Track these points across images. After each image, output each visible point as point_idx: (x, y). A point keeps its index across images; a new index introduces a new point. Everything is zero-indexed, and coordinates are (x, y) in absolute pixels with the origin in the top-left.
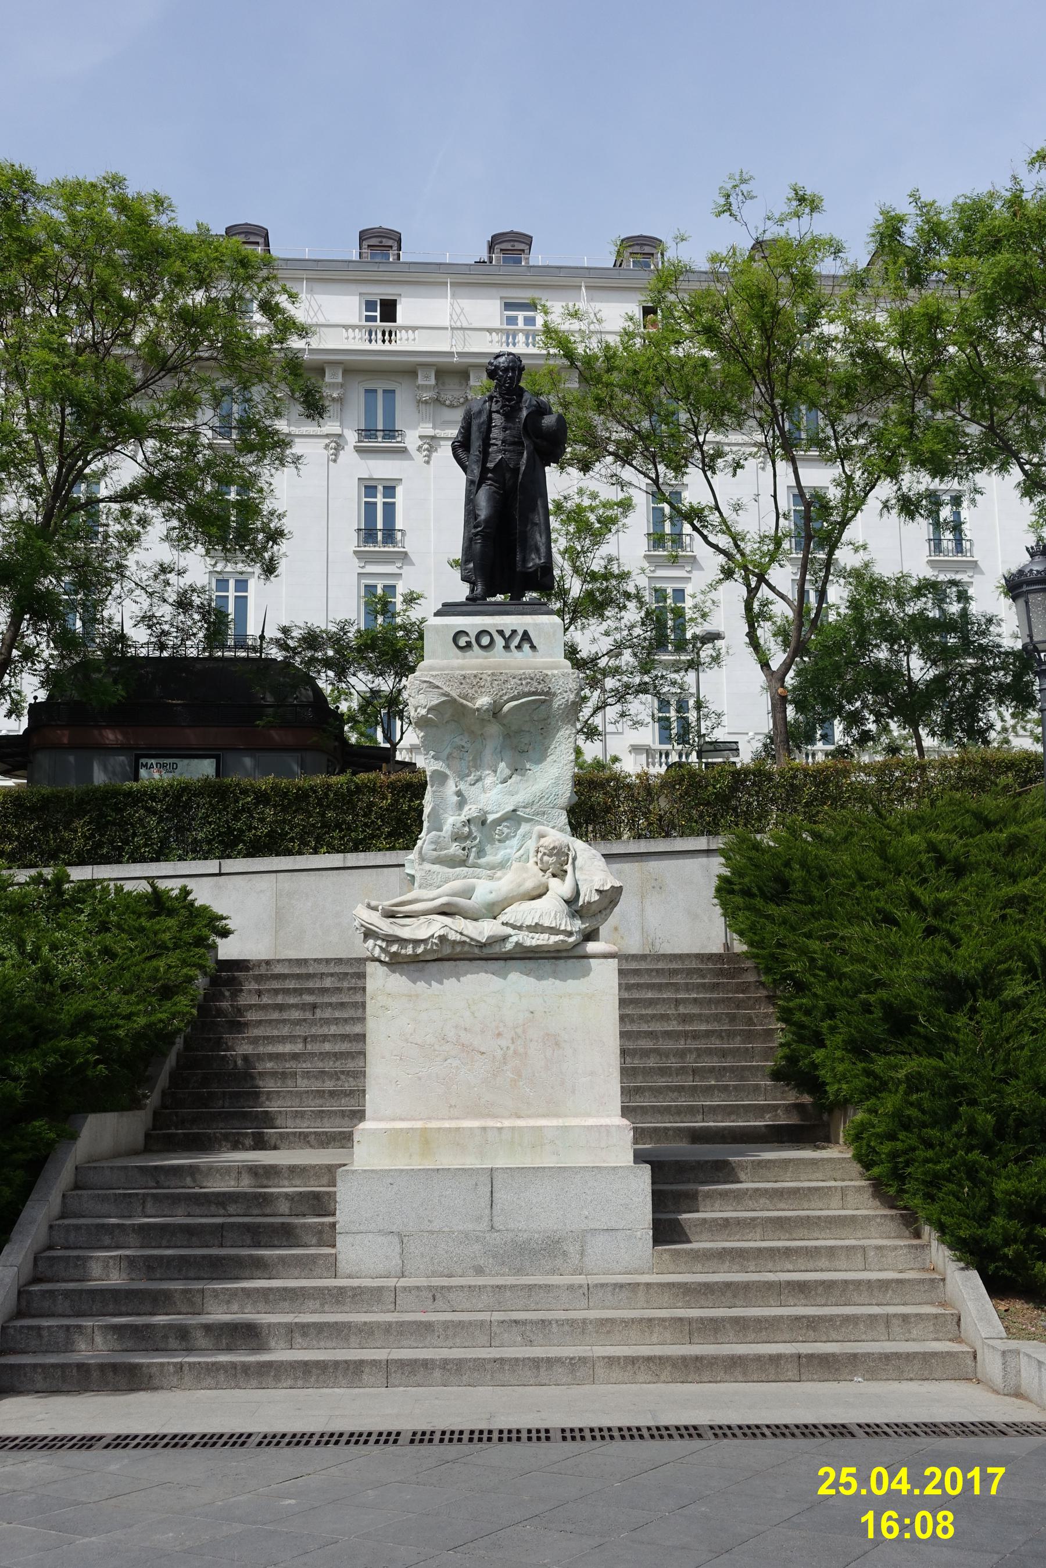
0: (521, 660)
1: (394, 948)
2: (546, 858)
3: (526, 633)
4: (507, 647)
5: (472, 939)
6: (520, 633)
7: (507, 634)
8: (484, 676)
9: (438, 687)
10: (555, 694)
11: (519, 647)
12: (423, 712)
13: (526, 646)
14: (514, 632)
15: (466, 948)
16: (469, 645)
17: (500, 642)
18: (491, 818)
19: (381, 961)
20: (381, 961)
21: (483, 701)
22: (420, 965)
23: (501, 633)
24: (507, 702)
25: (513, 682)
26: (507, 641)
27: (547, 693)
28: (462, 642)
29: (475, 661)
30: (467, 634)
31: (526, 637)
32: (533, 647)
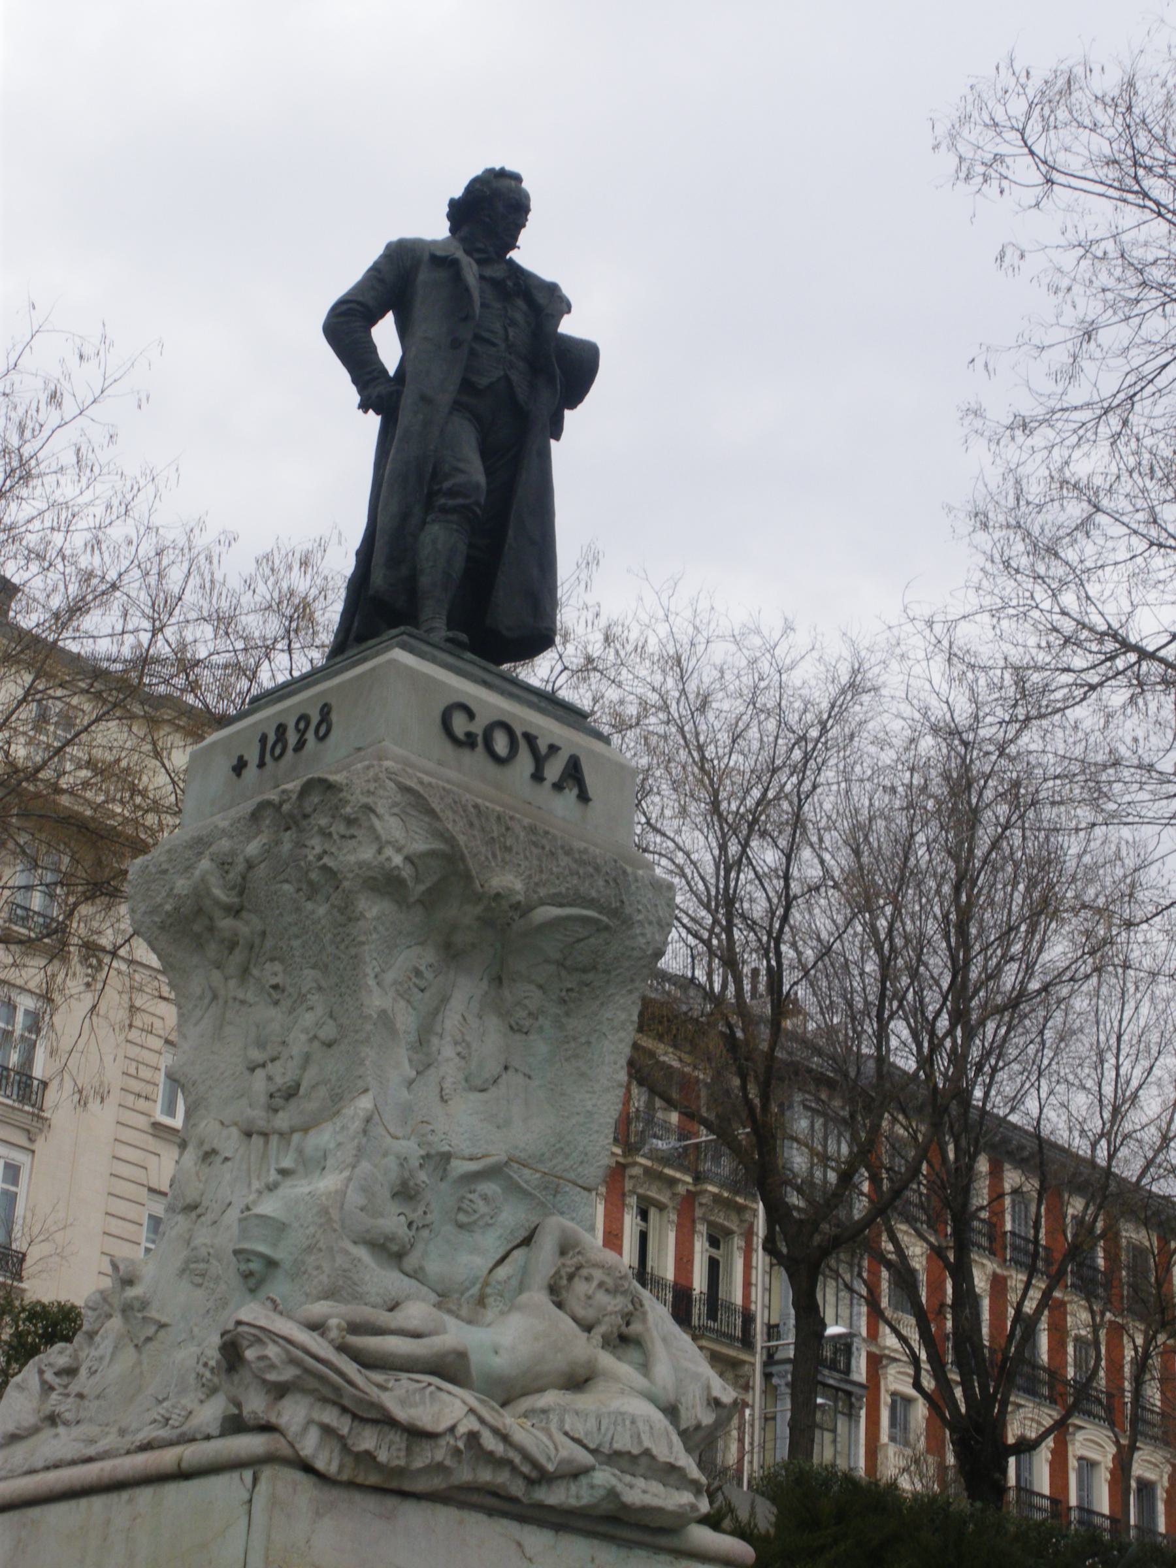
1: (367, 1440)
2: (602, 1298)
4: (538, 777)
5: (527, 1457)
8: (517, 828)
9: (431, 813)
10: (628, 922)
11: (558, 787)
12: (398, 860)
13: (571, 794)
15: (503, 1478)
16: (469, 741)
17: (525, 762)
18: (460, 1167)
19: (307, 1468)
20: (307, 1468)
21: (507, 881)
22: (391, 1502)
23: (530, 739)
24: (542, 903)
25: (564, 861)
26: (539, 761)
27: (615, 913)
30: (471, 715)
32: (584, 797)
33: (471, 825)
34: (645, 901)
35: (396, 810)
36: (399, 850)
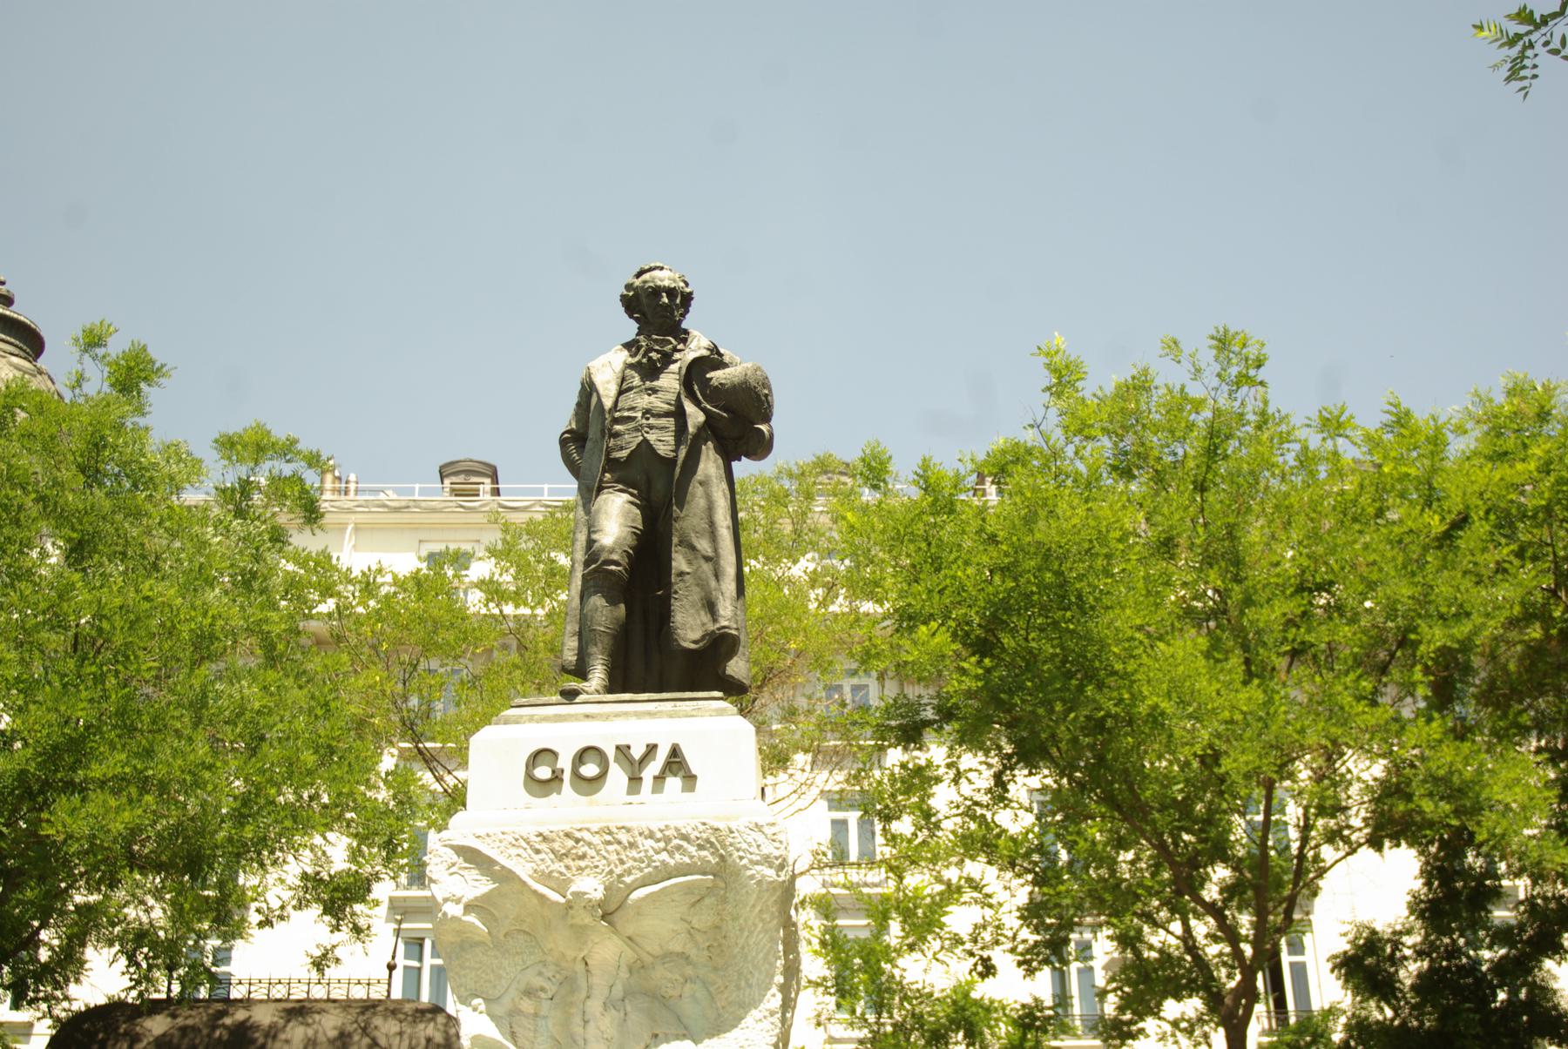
0: (667, 808)
3: (675, 751)
4: (635, 781)
6: (662, 755)
7: (637, 753)
11: (659, 779)
14: (652, 749)
16: (557, 777)
23: (623, 751)
24: (632, 888)
28: (543, 772)
29: (566, 809)
30: (555, 754)
31: (676, 762)
32: (690, 779)
33: (538, 852)
34: (744, 846)
35: (453, 869)
36: (458, 901)
